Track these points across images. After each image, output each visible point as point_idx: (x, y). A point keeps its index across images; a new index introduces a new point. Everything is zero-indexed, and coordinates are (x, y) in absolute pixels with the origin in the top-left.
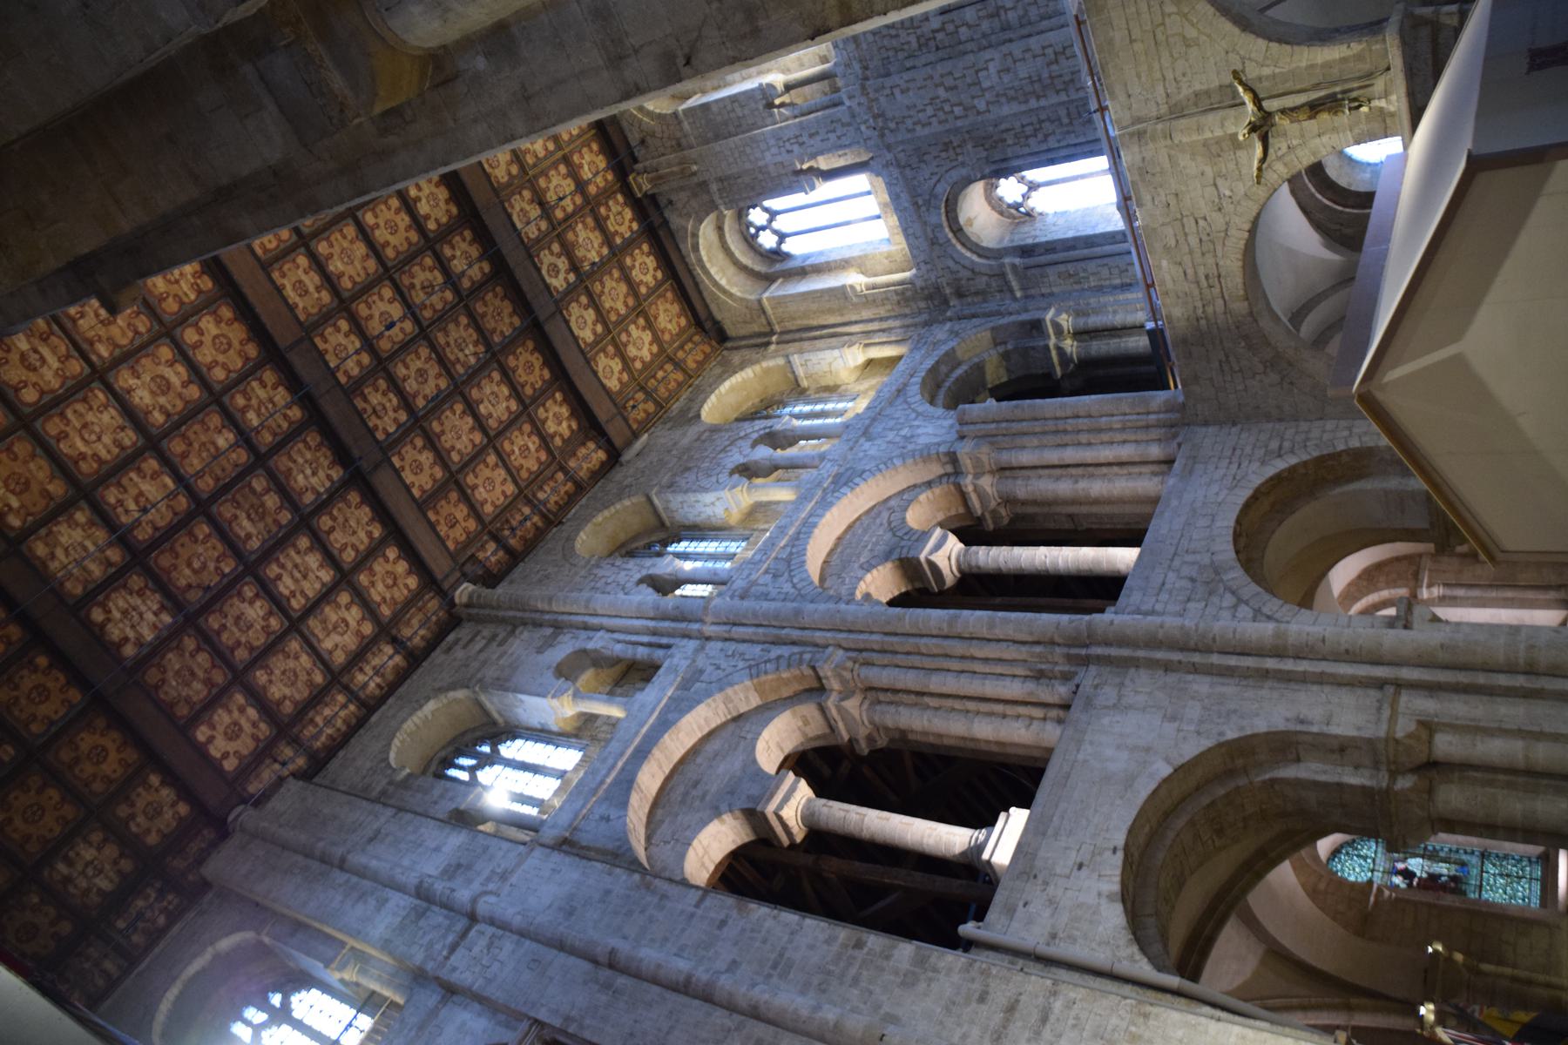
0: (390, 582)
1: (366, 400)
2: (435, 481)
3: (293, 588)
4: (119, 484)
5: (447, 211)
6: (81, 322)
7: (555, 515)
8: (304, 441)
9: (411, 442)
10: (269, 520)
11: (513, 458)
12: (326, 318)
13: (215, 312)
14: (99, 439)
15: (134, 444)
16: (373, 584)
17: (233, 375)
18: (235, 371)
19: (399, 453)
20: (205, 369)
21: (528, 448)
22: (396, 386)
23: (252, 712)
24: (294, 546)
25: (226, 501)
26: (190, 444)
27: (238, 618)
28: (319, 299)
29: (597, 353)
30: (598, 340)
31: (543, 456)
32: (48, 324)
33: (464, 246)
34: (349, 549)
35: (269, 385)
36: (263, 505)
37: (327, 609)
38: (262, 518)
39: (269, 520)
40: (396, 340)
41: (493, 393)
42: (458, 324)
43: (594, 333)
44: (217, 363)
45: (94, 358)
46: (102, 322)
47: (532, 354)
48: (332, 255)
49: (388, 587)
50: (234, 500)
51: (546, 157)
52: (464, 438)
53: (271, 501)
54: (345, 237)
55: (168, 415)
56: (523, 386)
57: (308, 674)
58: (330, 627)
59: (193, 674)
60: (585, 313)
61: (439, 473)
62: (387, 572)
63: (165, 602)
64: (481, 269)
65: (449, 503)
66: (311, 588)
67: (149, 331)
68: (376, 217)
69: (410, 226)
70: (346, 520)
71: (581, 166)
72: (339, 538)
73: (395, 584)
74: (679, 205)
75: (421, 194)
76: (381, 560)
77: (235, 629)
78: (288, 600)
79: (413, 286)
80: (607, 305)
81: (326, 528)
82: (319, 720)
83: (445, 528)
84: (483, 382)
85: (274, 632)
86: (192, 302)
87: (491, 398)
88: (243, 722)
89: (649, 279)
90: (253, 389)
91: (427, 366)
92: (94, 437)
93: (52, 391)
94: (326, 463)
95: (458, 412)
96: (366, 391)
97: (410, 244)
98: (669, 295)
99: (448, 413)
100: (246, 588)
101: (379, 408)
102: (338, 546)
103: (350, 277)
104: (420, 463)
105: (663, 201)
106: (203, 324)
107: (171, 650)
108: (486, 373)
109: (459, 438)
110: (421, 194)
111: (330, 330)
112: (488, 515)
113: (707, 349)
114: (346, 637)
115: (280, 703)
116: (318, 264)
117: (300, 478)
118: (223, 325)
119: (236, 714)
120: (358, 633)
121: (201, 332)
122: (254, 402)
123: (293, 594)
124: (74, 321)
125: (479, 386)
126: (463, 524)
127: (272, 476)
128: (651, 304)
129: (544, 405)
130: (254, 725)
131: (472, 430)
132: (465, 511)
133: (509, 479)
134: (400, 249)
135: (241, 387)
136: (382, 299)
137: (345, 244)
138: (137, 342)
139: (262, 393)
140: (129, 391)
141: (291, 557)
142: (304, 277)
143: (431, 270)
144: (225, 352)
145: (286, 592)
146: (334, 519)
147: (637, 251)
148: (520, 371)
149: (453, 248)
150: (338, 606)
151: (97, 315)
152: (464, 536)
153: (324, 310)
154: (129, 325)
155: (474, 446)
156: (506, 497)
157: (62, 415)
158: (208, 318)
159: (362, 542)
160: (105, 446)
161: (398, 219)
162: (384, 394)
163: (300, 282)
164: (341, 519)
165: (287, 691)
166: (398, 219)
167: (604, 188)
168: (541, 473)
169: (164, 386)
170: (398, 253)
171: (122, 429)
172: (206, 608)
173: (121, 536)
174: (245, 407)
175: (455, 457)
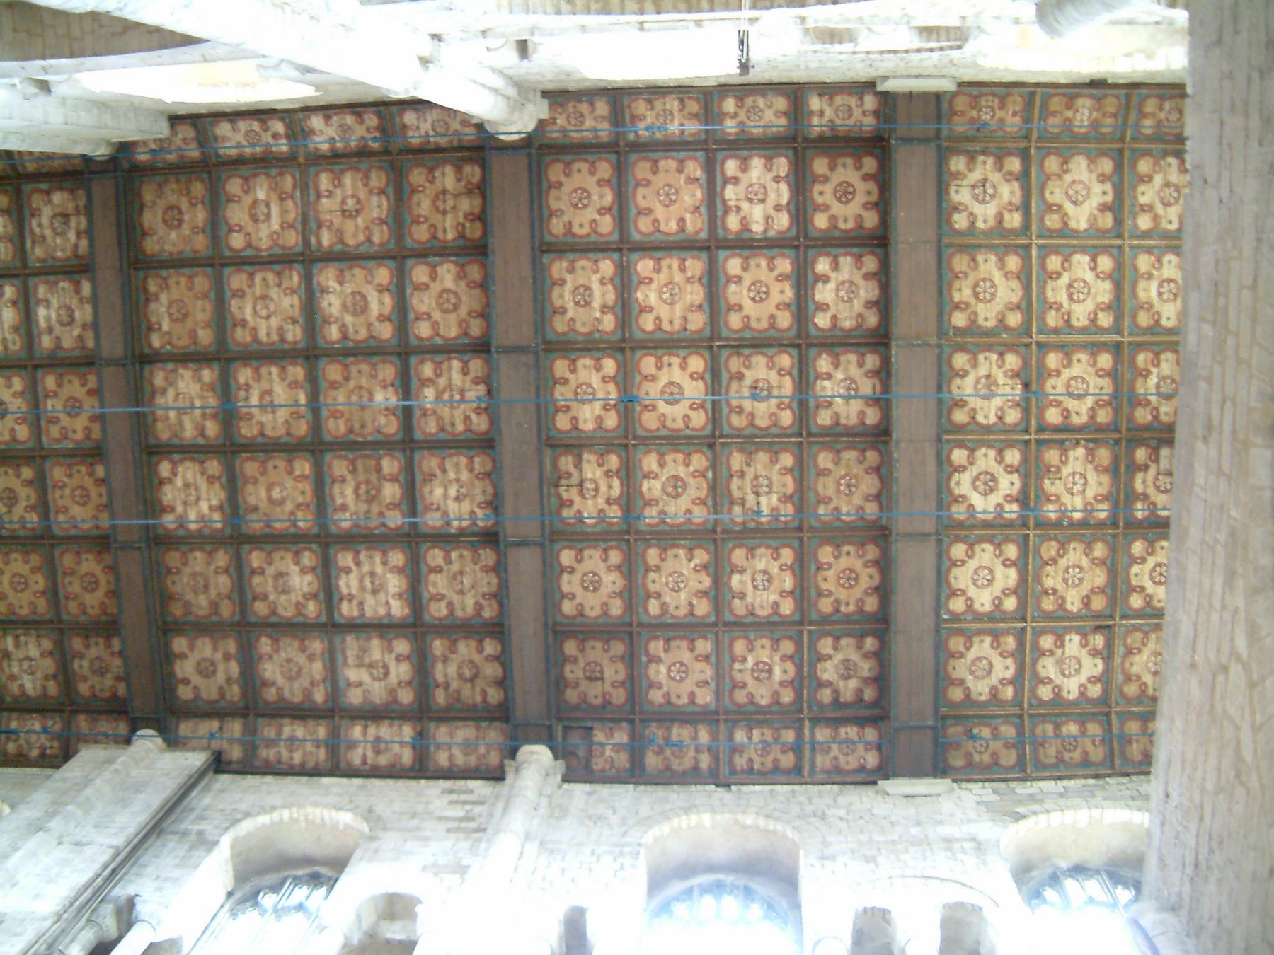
1: (578, 465)
2: (605, 614)
3: (354, 592)
4: (257, 370)
5: (860, 315)
6: (324, 201)
7: (733, 771)
8: (471, 459)
9: (605, 550)
10: (375, 509)
11: (737, 666)
12: (592, 346)
13: (463, 266)
14: (268, 317)
15: (295, 343)
16: (445, 660)
17: (438, 341)
19: (580, 551)
21: (770, 671)
22: (628, 474)
23: (234, 668)
24: (384, 553)
25: (344, 457)
26: (347, 379)
27: (280, 575)
29: (980, 632)
30: (997, 615)
32: (295, 186)
33: (855, 372)
34: (443, 604)
35: (472, 374)
36: (379, 490)
37: (375, 643)
38: (371, 500)
39: (375, 509)
40: (669, 424)
44: (429, 316)
45: (313, 240)
46: (343, 211)
47: (865, 565)
48: (651, 280)
49: (460, 676)
50: (353, 462)
51: (1083, 330)
52: (683, 596)
53: (391, 491)
54: (683, 270)
55: (345, 337)
56: (820, 594)
57: (312, 684)
58: (367, 661)
59: (206, 587)
60: (999, 571)
61: (616, 609)
62: (472, 662)
63: (226, 506)
64: (862, 414)
65: (606, 651)
66: (374, 608)
67: (382, 244)
68: (745, 269)
69: (788, 306)
70: (461, 573)
72: (440, 583)
75: (833, 275)
76: (473, 644)
77: (270, 580)
78: (341, 599)
79: (740, 377)
80: (1049, 583)
81: (432, 564)
82: (287, 731)
83: (580, 674)
85: (304, 616)
86: (445, 241)
87: (759, 577)
88: (221, 668)
90: (450, 368)
91: (691, 481)
92: (264, 313)
93: (258, 249)
94: (480, 498)
95: (696, 561)
96: (586, 456)
97: (772, 326)
99: (681, 552)
100: (307, 554)
102: (433, 590)
103: (658, 318)
104: (600, 581)
106: (441, 270)
107: (202, 550)
108: (774, 543)
110: (833, 275)
111: (588, 362)
114: (376, 684)
115: (265, 683)
116: (625, 283)
117: (439, 492)
118: (463, 283)
119: (218, 656)
120: (392, 692)
121: (433, 277)
122: (442, 382)
123: (351, 598)
124: (319, 196)
125: (751, 550)
126: (608, 688)
127: (409, 468)
128: (1135, 629)
129: (837, 638)
130: (229, 680)
132: (622, 676)
133: (713, 685)
134: (754, 324)
135: (438, 358)
136: (683, 367)
137: (678, 278)
138: (363, 249)
139: (457, 378)
140: (324, 291)
141: (373, 561)
142: (596, 286)
143: (781, 372)
144: (446, 311)
145: (345, 591)
146: (448, 561)
148: (831, 574)
149: (836, 366)
150: (390, 650)
151: (343, 202)
152: (599, 701)
153: (597, 335)
154: (367, 228)
156: (692, 702)
157: (251, 276)
158: (452, 267)
159: (463, 609)
160: (269, 328)
161: (775, 288)
162: (608, 474)
163: (588, 288)
164: (455, 567)
165: (280, 681)
166: (775, 288)
168: (765, 713)
169: (359, 306)
170: (747, 327)
171: (294, 321)
172: (258, 541)
173: (228, 416)
174: (429, 380)
175: (653, 607)
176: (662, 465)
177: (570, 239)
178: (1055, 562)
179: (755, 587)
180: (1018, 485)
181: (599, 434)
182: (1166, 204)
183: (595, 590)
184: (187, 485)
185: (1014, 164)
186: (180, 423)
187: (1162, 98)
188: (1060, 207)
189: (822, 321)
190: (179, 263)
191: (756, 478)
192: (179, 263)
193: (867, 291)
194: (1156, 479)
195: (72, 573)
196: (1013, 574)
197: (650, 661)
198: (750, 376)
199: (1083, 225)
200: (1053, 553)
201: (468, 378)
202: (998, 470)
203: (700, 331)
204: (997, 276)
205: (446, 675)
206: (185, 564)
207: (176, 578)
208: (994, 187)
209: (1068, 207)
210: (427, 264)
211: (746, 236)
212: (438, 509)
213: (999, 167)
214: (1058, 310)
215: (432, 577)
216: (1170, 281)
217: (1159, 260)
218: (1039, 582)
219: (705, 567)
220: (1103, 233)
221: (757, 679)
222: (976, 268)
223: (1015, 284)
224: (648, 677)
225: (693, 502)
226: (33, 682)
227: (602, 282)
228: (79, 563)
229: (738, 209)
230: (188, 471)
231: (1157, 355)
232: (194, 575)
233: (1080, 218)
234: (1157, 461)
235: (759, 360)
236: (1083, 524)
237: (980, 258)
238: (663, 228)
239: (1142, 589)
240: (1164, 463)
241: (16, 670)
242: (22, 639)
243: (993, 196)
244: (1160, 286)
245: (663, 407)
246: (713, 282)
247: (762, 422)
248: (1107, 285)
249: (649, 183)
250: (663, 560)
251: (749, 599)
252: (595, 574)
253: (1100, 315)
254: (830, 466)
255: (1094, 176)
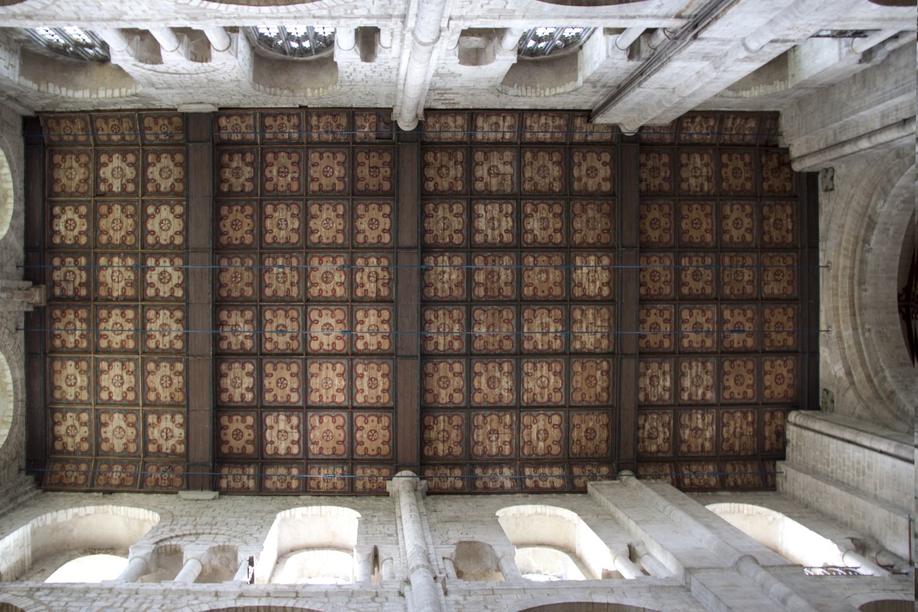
0: (444, 170)
1: (378, 290)
2: (367, 206)
3: (504, 219)
4: (550, 347)
5: (230, 370)
8: (435, 295)
9: (365, 242)
10: (489, 267)
11: (296, 175)
12: (368, 355)
14: (541, 377)
15: (527, 362)
16: (456, 178)
17: (450, 361)
18: (448, 363)
20: (464, 375)
21: (279, 172)
22: (352, 285)
23: (576, 173)
24: (486, 241)
25: (505, 297)
26: (500, 341)
27: (545, 229)
28: (365, 370)
29: (166, 194)
31: (270, 157)
33: (232, 339)
34: (455, 211)
35: (433, 342)
36: (487, 278)
37: (494, 189)
38: (493, 271)
39: (489, 267)
40: (330, 313)
41: (280, 229)
42: (275, 291)
43: (158, 210)
45: (514, 418)
46: (498, 433)
47: (227, 233)
48: (337, 391)
49: (448, 169)
50: (500, 294)
51: (115, 360)
52: (325, 216)
53: (480, 277)
54: (321, 396)
55: (500, 364)
57: (532, 163)
58: (500, 177)
59: (588, 221)
60: (156, 228)
62: (441, 177)
63: (573, 270)
64: (229, 317)
65: (367, 184)
66: (494, 209)
67: (477, 414)
68: (289, 396)
69: (267, 376)
70: (444, 229)
71: (82, 336)
73: (442, 166)
74: (13, 260)
75: (244, 391)
76: (440, 188)
77: (551, 225)
78: (512, 214)
79: (292, 338)
82: (548, 135)
84: (282, 241)
85: (533, 204)
86: (444, 415)
88: (584, 172)
89: (70, 214)
90: (444, 345)
91: (318, 281)
92: (544, 379)
93: (545, 414)
94: (432, 272)
95: (317, 236)
96: (374, 295)
97: (275, 365)
98: (57, 189)
99: (325, 241)
100: (529, 241)
101: (373, 279)
103: (334, 370)
104: (369, 224)
105: (21, 271)
106: (447, 400)
107: (588, 244)
109: (328, 219)
110: (244, 391)
112: (344, 154)
113: (52, 124)
114: (495, 163)
115: (558, 163)
116: (351, 389)
117: (454, 277)
118: (436, 392)
119: (584, 180)
120: (487, 159)
121: (451, 396)
122: (449, 338)
123: (506, 216)
125: (288, 241)
126: (367, 162)
127: (470, 290)
128: (83, 194)
129: (243, 191)
130: (580, 165)
131: (314, 217)
132: (359, 169)
133: (310, 164)
134: (285, 366)
136: (322, 344)
138: (488, 412)
139: (441, 340)
140: (510, 390)
141: (492, 236)
142: (366, 388)
143: (271, 340)
144: (445, 377)
145: (509, 219)
146: (451, 236)
147: (68, 242)
148: (246, 228)
149: (242, 343)
150: (486, 184)
151: (497, 438)
152: (372, 154)
153: (366, 362)
154: (485, 424)
155: (320, 206)
156: (321, 154)
157: (549, 400)
158: (441, 401)
160: (542, 371)
161: (273, 385)
162: (363, 285)
163: (370, 387)
164: (447, 233)
165: (550, 165)
167: (69, 307)
169: (492, 382)
170: (288, 365)
171: (527, 374)
172: (557, 248)
173: (568, 322)
174: (456, 339)
175: (340, 210)
176: (334, 290)
177: (379, 414)
178: (127, 233)
179: (286, 220)
180: (148, 276)
181: (367, 307)
182: (72, 426)
183: (372, 220)
184: (594, 282)
185: (152, 448)
186: (595, 318)
187: (75, 484)
188: (128, 425)
189: (249, 367)
190: (589, 408)
191: (284, 282)
192: (589, 408)
193: (227, 382)
194: (75, 278)
195: (664, 230)
196: (150, 227)
197: (343, 178)
198: (287, 338)
199: (116, 415)
200: (128, 238)
201: (435, 340)
202: (159, 285)
203: (312, 363)
204: (160, 390)
205: (456, 169)
206: (599, 235)
207: (605, 226)
208: (162, 437)
209: (124, 425)
210: (454, 403)
211: (288, 413)
212: (454, 267)
213: (159, 447)
214: (128, 371)
215: (460, 227)
216: (71, 386)
217: (76, 396)
218: (136, 222)
219: (312, 232)
220: (105, 412)
221: (285, 168)
222: (171, 394)
223: (151, 385)
224: (345, 169)
225: (318, 269)
226: (695, 162)
227: (363, 390)
228: (661, 236)
229: (292, 428)
230: (592, 290)
231: (76, 346)
232: (594, 229)
233: (118, 420)
234: (75, 289)
235: (282, 346)
236: (113, 255)
237: (169, 399)
238: (331, 419)
239: (80, 217)
240: (72, 288)
241: (705, 170)
242: (698, 190)
243: (162, 431)
244: (75, 383)
245: (332, 322)
246: (305, 389)
247: (281, 312)
248: (103, 384)
249: (337, 442)
250: (335, 236)
251: (289, 213)
252: (371, 228)
253: (106, 368)
254: (246, 288)
255: (111, 441)
